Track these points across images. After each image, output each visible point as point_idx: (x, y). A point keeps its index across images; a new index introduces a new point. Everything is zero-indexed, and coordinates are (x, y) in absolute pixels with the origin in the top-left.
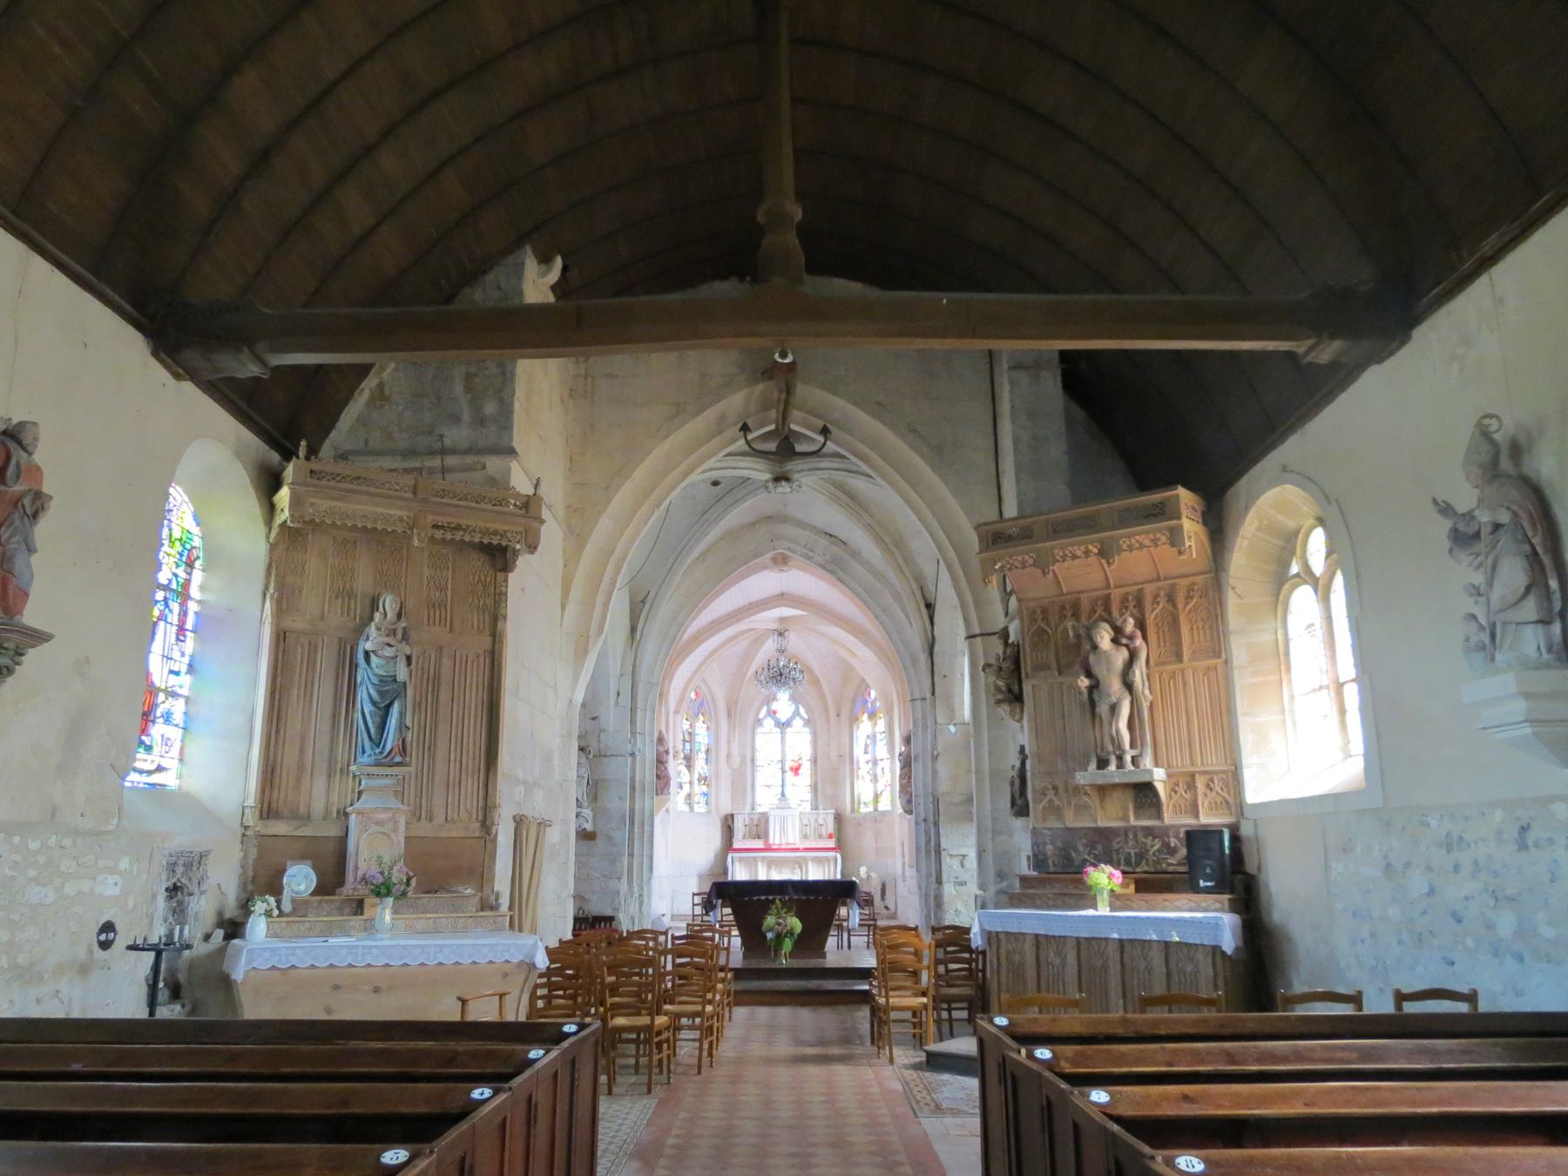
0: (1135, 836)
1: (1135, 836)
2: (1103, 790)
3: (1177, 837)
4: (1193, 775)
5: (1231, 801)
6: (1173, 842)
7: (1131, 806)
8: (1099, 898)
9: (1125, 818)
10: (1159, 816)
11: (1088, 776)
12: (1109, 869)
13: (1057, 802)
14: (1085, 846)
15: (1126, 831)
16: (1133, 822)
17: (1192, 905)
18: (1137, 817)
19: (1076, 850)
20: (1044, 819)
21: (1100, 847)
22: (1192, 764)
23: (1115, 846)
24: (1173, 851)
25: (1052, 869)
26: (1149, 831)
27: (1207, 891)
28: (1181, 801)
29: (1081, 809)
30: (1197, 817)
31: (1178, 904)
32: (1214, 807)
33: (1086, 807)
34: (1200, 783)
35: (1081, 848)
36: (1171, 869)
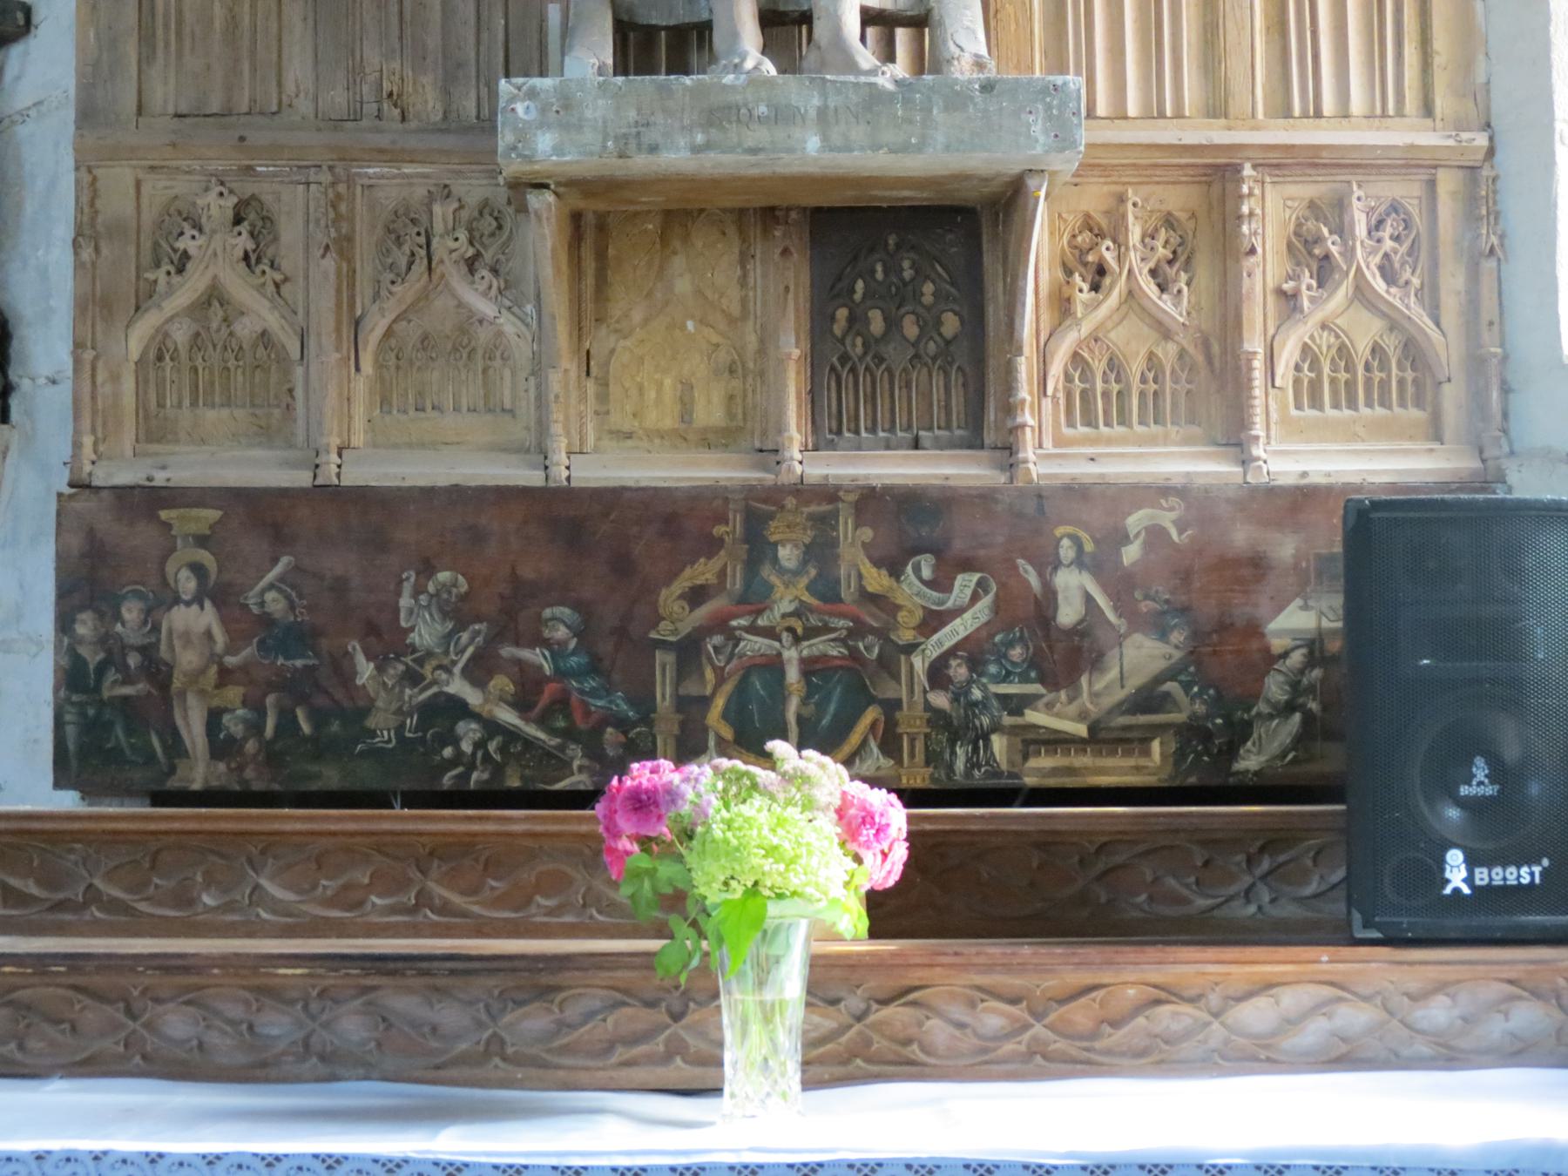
0: (821, 551)
1: (821, 551)
2: (613, 225)
3: (1099, 564)
4: (1218, 176)
5: (1445, 345)
6: (1074, 592)
7: (792, 348)
8: (737, 1004)
9: (748, 430)
10: (981, 416)
11: (571, 111)
12: (828, 777)
13: (259, 312)
14: (458, 613)
15: (758, 511)
16: (804, 463)
17: (1354, 1017)
18: (829, 430)
19: (386, 640)
20: (154, 431)
21: (560, 624)
22: (1217, 108)
23: (677, 618)
24: (1065, 656)
25: (198, 773)
26: (909, 521)
27: (1485, 923)
28: (1133, 343)
29: (423, 361)
30: (1234, 438)
31: (1256, 1015)
32: (1333, 382)
33: (462, 344)
34: (1269, 213)
35: (426, 633)
36: (1039, 769)
